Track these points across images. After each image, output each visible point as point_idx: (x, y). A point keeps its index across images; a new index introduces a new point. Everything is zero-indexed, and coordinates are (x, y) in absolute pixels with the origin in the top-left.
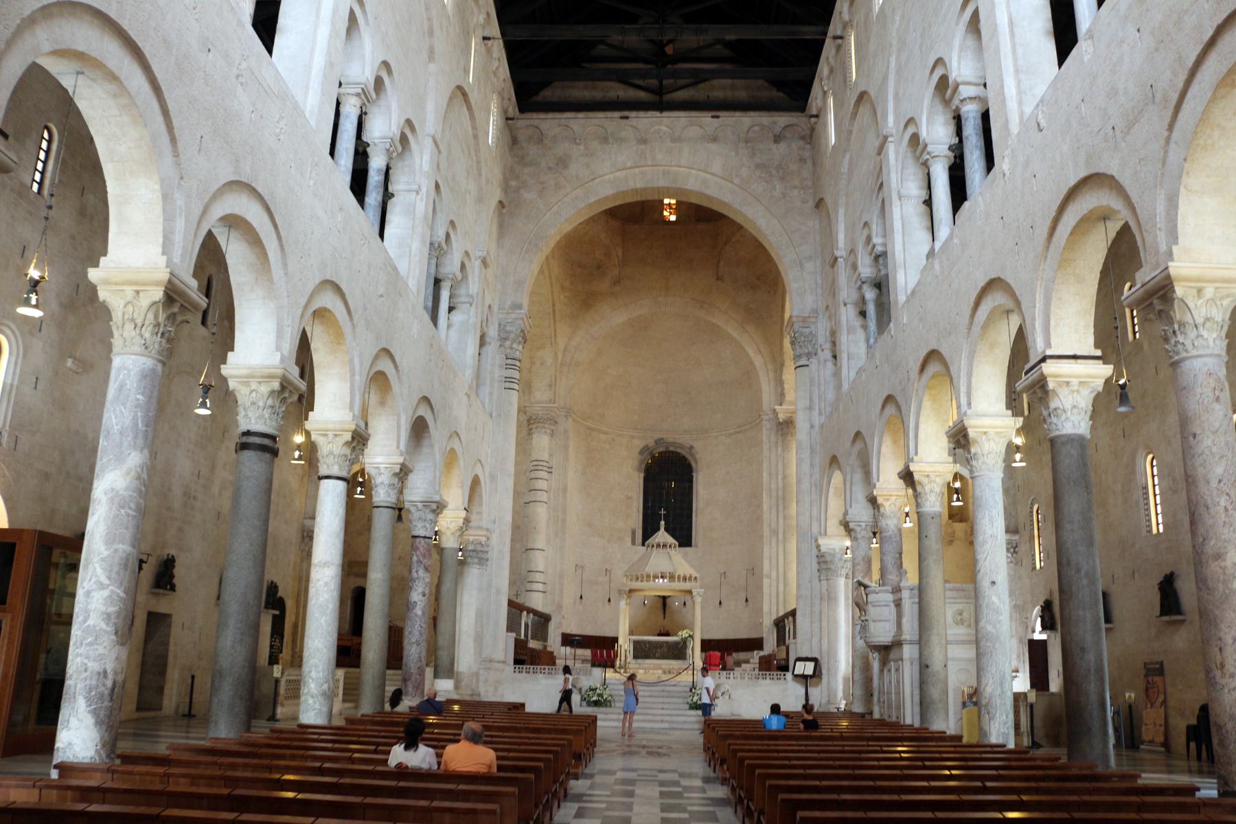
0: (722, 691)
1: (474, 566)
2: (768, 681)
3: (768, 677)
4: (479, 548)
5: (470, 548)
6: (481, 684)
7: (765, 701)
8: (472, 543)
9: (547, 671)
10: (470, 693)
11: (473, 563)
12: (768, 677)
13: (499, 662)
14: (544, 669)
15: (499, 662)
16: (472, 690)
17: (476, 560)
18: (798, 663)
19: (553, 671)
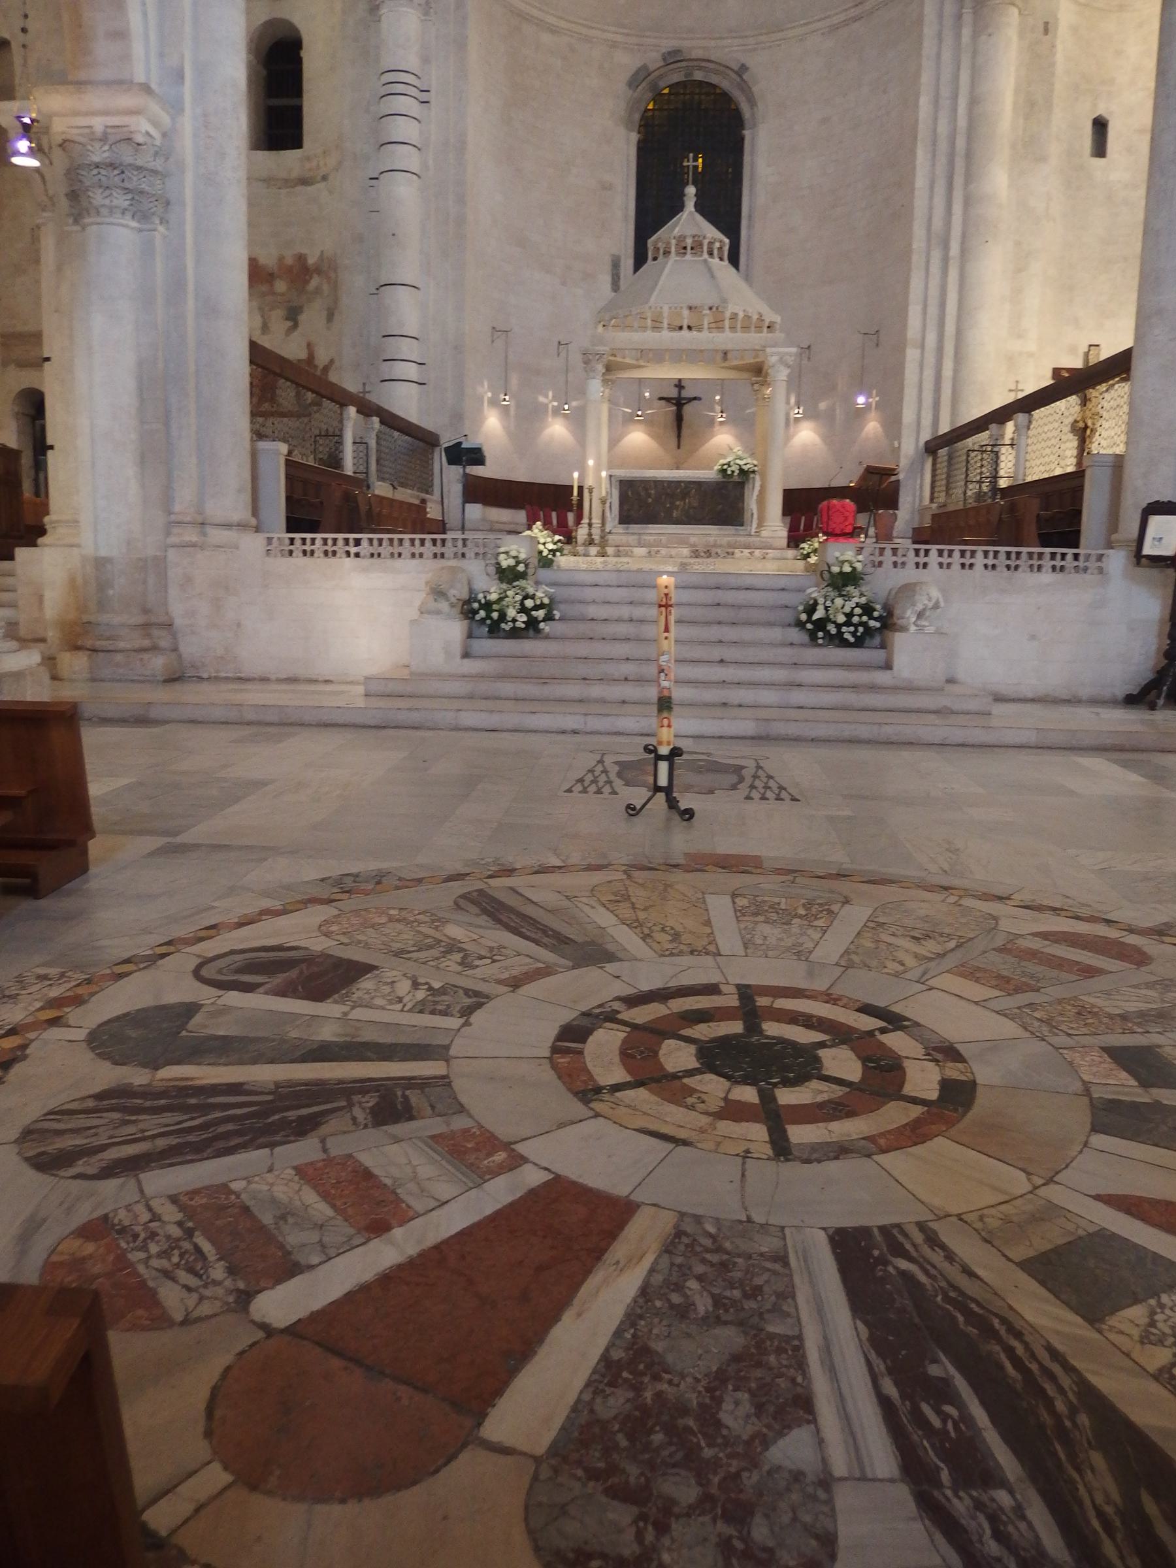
0: (920, 607)
1: (117, 218)
2: (1047, 577)
3: (1047, 563)
4: (126, 155)
5: (96, 158)
6: (173, 592)
7: (1033, 637)
8: (104, 139)
9: (365, 548)
10: (140, 619)
11: (111, 210)
12: (1047, 563)
13: (228, 526)
14: (358, 542)
15: (228, 526)
16: (146, 611)
17: (121, 201)
18: (1155, 521)
19: (385, 550)
